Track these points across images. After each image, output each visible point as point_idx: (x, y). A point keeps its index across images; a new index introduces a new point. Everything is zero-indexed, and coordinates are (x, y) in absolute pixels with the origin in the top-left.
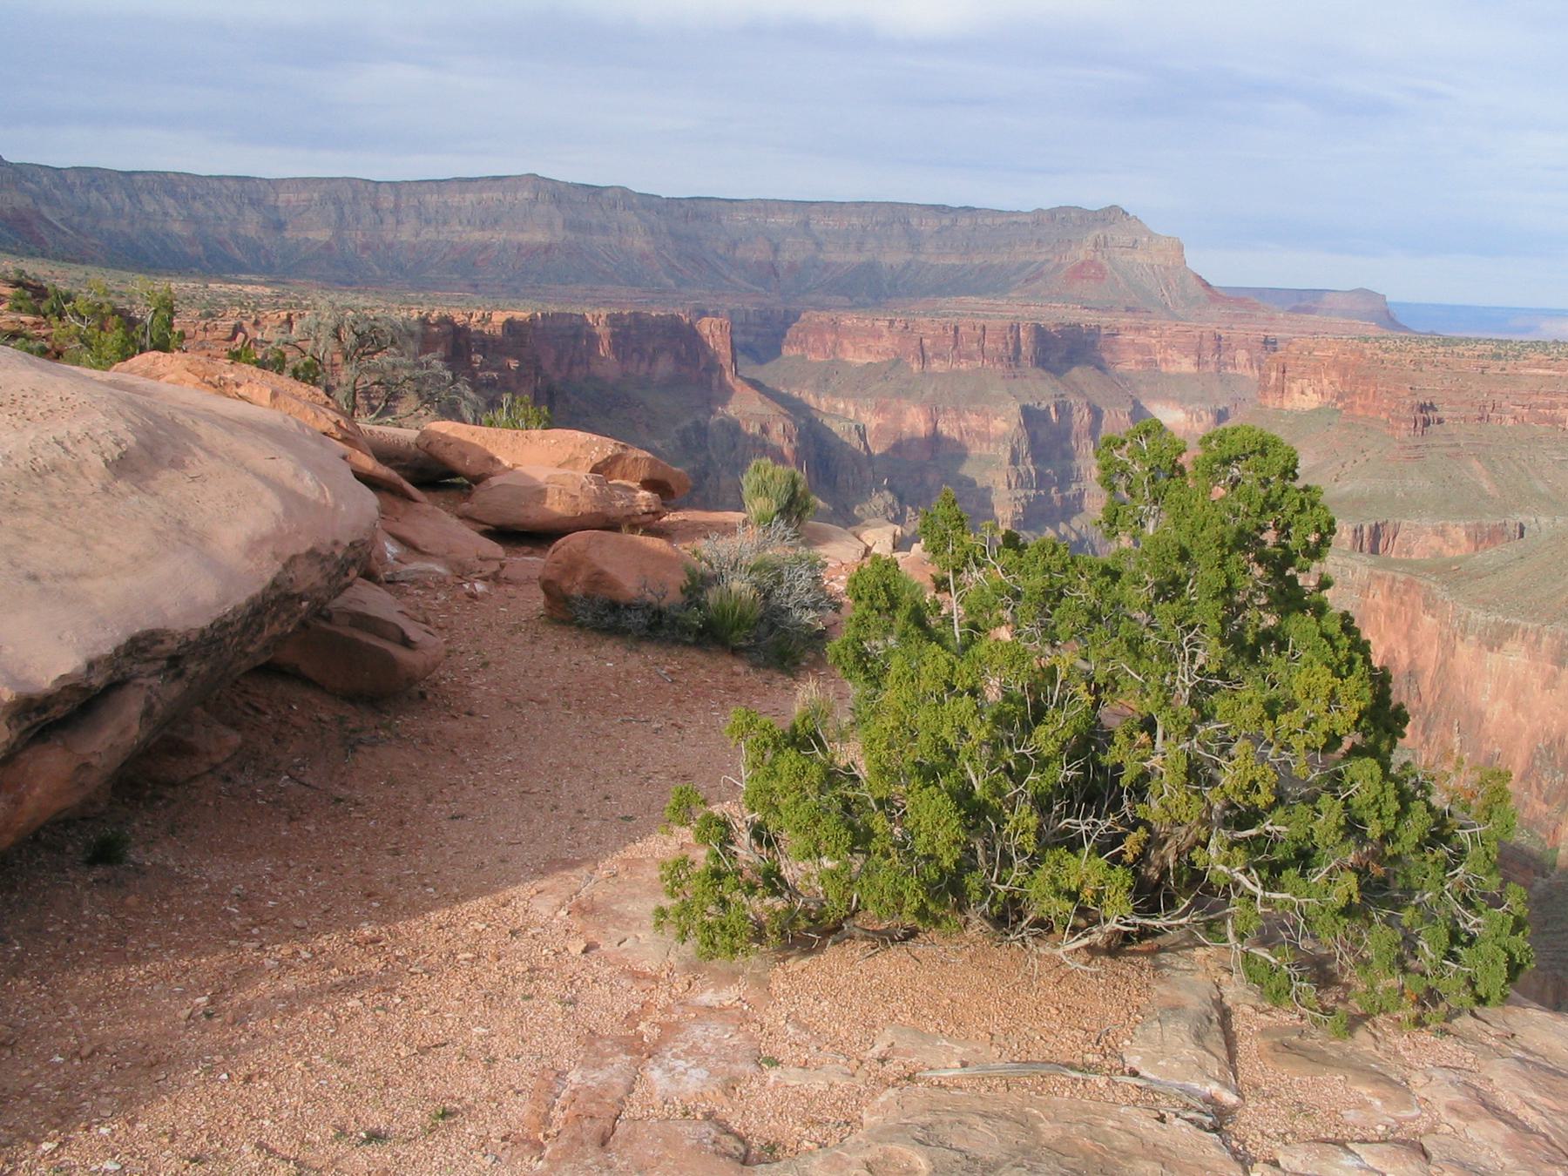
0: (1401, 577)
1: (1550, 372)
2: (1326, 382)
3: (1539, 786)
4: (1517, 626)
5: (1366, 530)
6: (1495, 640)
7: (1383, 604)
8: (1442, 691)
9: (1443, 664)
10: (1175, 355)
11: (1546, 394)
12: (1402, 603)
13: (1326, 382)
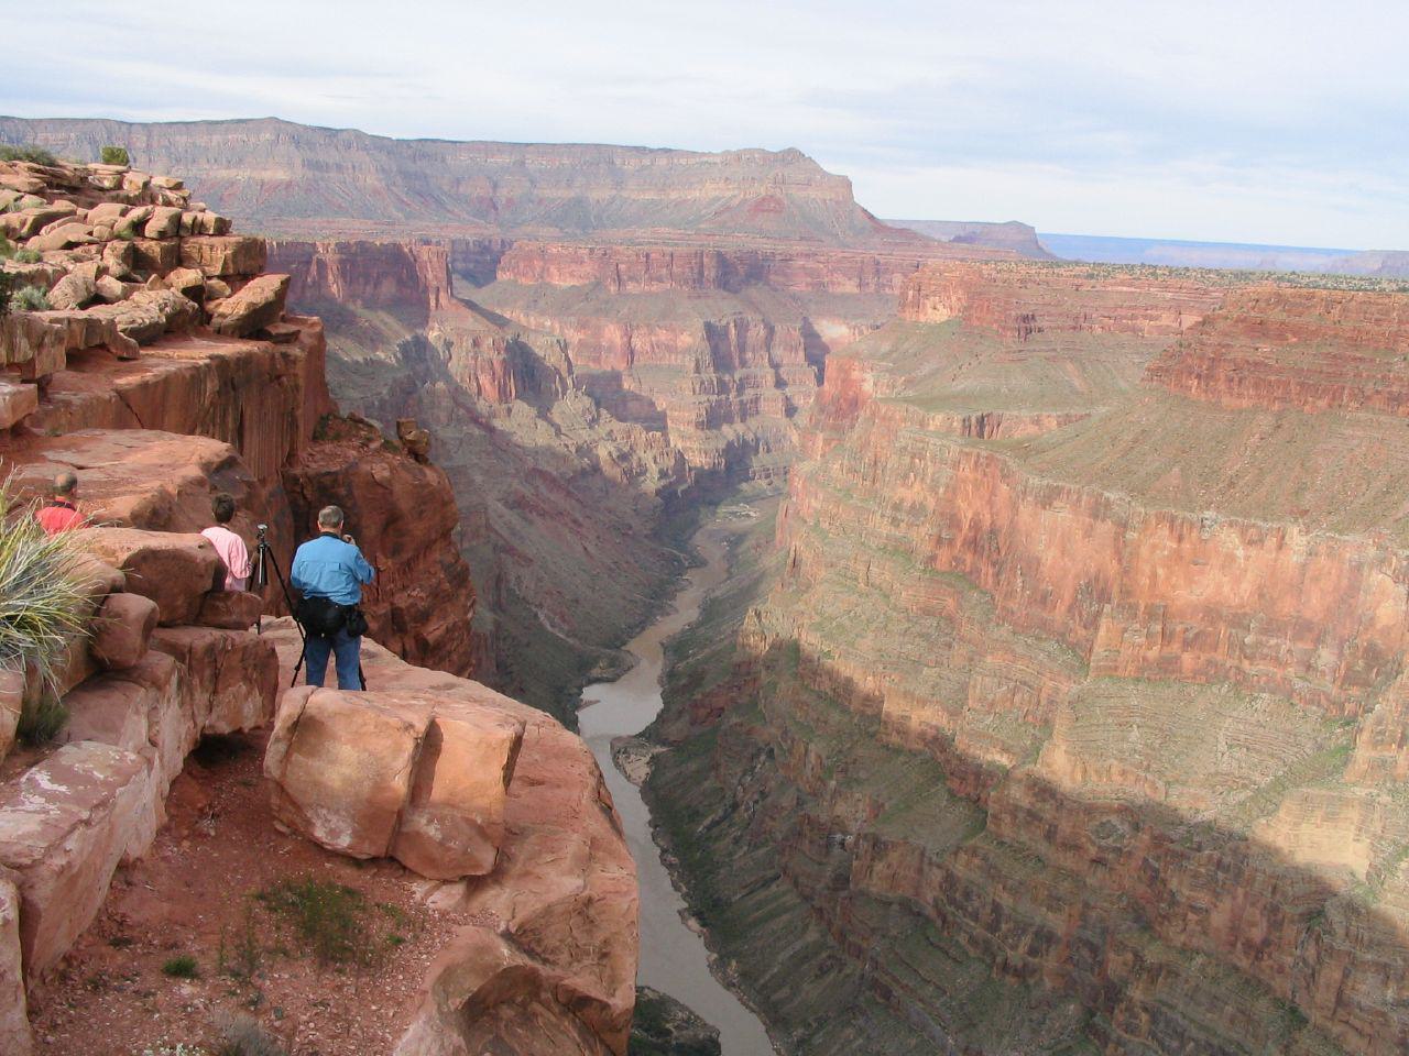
0: (984, 453)
1: (1133, 289)
2: (954, 299)
3: (1080, 615)
4: (1063, 488)
5: (973, 420)
6: (1047, 499)
7: (971, 476)
8: (1010, 543)
9: (1011, 522)
10: (841, 279)
11: (1130, 308)
12: (985, 475)
13: (954, 299)
